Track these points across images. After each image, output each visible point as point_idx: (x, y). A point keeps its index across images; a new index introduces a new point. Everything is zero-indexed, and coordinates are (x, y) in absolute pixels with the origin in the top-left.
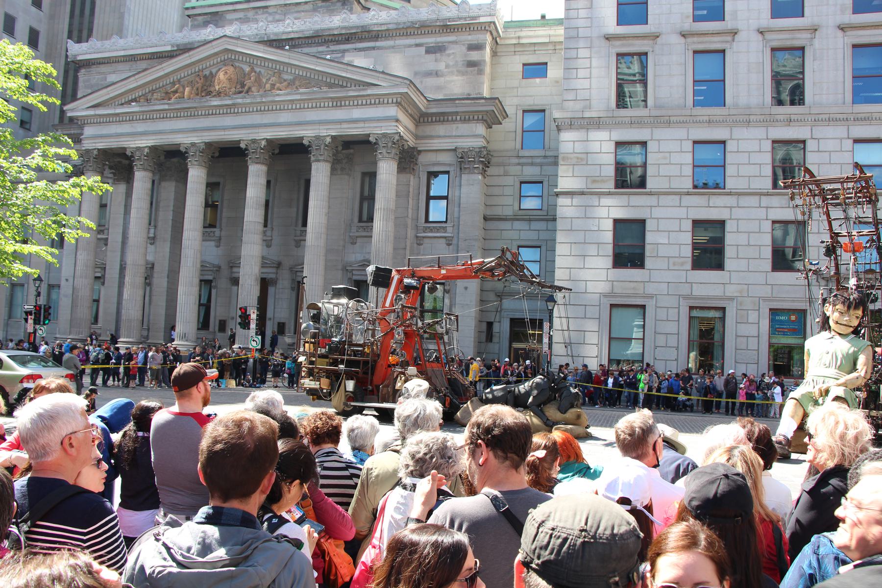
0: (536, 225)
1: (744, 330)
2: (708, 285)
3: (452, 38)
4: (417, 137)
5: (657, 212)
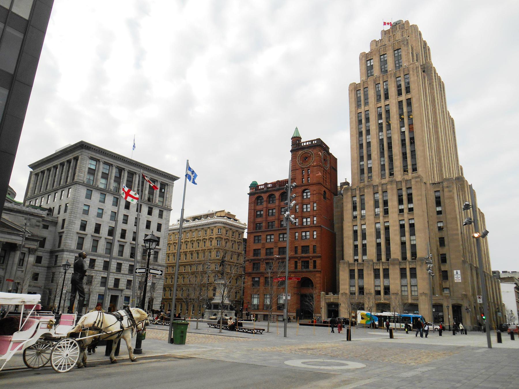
0: (39, 268)
3: (33, 217)
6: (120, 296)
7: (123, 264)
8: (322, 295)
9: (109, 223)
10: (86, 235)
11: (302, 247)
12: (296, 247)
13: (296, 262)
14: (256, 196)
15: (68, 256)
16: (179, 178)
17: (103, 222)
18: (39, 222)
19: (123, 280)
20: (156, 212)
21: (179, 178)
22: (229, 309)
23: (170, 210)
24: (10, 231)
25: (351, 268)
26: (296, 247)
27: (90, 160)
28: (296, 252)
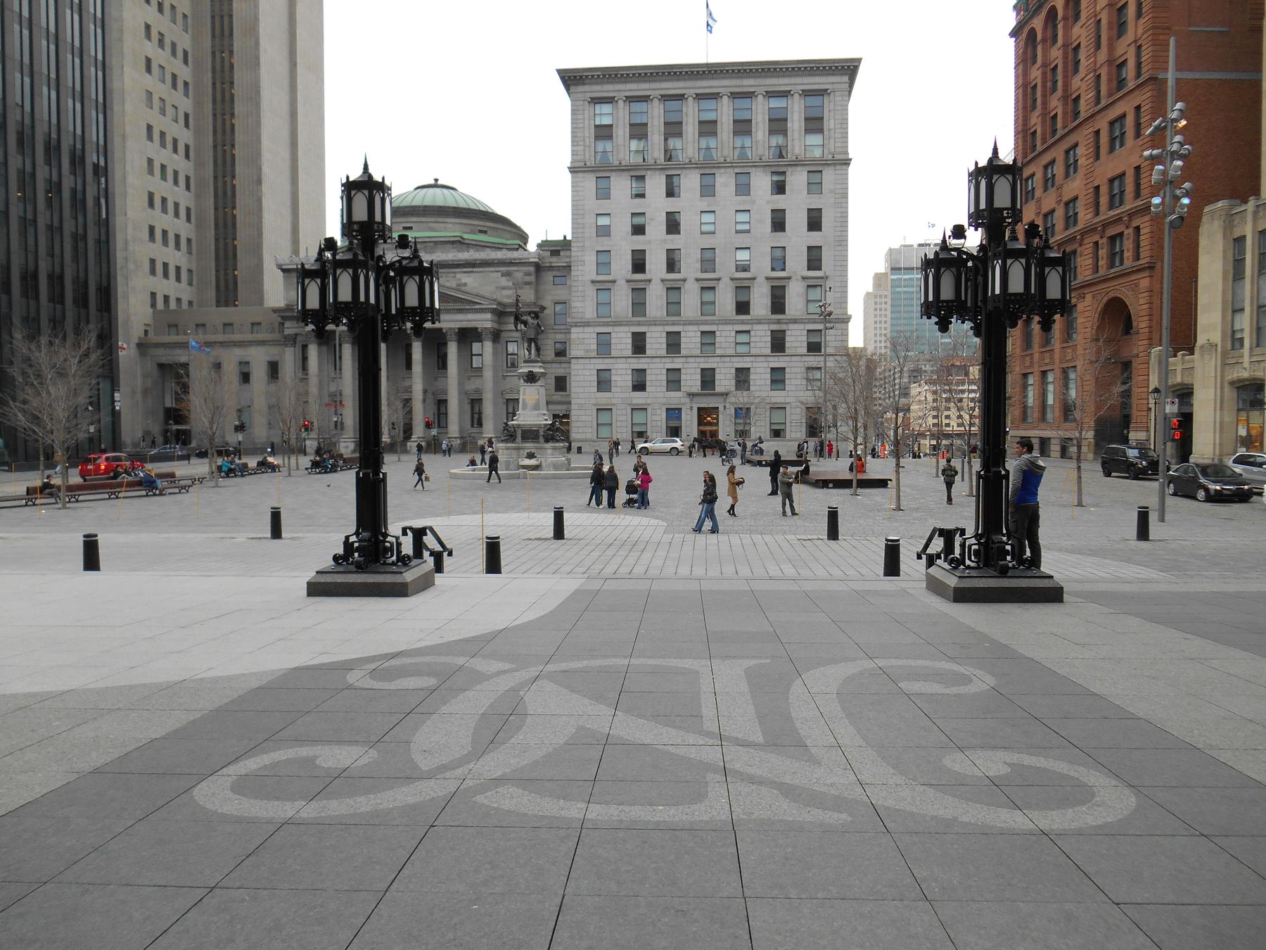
1: (655, 418)
2: (639, 398)
4: (499, 323)
5: (616, 366)
6: (721, 409)
7: (718, 334)
8: (1153, 360)
9: (665, 241)
10: (614, 282)
11: (1111, 181)
12: (1097, 188)
13: (1096, 243)
14: (1026, 31)
15: (581, 336)
16: (859, 60)
17: (649, 242)
18: (528, 274)
19: (723, 371)
20: (797, 180)
21: (859, 60)
22: (542, 439)
23: (847, 162)
24: (458, 306)
25: (1237, 234)
26: (1097, 188)
27: (598, 106)
28: (1097, 213)
